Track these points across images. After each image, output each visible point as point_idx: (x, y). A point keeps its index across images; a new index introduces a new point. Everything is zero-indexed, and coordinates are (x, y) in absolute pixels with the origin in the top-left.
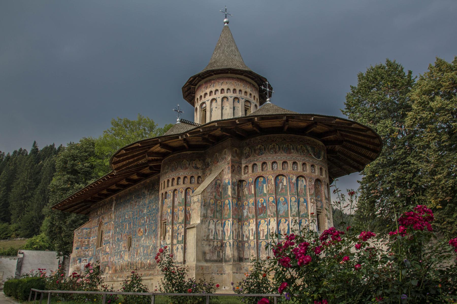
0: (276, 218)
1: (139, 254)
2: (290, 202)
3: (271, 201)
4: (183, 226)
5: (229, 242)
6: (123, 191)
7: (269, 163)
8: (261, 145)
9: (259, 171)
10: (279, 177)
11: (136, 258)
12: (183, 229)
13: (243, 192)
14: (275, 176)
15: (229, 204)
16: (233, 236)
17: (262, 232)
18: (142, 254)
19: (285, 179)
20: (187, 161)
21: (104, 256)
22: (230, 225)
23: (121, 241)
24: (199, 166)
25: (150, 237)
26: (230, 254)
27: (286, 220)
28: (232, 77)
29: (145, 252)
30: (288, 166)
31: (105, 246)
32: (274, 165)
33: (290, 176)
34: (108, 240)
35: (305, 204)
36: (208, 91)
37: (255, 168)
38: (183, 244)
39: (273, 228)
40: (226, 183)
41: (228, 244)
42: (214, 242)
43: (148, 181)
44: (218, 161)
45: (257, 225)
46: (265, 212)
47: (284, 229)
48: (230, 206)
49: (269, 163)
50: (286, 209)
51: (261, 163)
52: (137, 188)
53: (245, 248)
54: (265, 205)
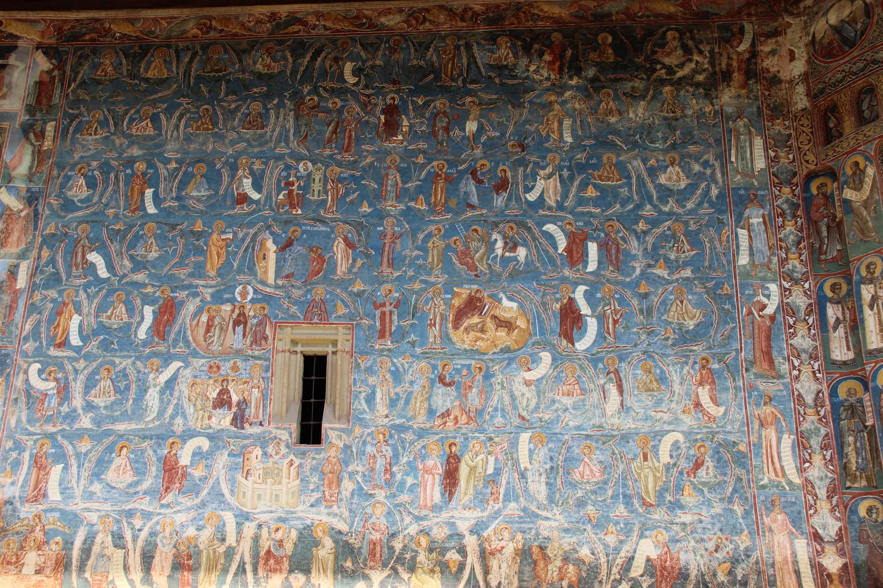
1: (492, 480)
11: (436, 508)
18: (538, 487)
23: (167, 359)
25: (632, 374)
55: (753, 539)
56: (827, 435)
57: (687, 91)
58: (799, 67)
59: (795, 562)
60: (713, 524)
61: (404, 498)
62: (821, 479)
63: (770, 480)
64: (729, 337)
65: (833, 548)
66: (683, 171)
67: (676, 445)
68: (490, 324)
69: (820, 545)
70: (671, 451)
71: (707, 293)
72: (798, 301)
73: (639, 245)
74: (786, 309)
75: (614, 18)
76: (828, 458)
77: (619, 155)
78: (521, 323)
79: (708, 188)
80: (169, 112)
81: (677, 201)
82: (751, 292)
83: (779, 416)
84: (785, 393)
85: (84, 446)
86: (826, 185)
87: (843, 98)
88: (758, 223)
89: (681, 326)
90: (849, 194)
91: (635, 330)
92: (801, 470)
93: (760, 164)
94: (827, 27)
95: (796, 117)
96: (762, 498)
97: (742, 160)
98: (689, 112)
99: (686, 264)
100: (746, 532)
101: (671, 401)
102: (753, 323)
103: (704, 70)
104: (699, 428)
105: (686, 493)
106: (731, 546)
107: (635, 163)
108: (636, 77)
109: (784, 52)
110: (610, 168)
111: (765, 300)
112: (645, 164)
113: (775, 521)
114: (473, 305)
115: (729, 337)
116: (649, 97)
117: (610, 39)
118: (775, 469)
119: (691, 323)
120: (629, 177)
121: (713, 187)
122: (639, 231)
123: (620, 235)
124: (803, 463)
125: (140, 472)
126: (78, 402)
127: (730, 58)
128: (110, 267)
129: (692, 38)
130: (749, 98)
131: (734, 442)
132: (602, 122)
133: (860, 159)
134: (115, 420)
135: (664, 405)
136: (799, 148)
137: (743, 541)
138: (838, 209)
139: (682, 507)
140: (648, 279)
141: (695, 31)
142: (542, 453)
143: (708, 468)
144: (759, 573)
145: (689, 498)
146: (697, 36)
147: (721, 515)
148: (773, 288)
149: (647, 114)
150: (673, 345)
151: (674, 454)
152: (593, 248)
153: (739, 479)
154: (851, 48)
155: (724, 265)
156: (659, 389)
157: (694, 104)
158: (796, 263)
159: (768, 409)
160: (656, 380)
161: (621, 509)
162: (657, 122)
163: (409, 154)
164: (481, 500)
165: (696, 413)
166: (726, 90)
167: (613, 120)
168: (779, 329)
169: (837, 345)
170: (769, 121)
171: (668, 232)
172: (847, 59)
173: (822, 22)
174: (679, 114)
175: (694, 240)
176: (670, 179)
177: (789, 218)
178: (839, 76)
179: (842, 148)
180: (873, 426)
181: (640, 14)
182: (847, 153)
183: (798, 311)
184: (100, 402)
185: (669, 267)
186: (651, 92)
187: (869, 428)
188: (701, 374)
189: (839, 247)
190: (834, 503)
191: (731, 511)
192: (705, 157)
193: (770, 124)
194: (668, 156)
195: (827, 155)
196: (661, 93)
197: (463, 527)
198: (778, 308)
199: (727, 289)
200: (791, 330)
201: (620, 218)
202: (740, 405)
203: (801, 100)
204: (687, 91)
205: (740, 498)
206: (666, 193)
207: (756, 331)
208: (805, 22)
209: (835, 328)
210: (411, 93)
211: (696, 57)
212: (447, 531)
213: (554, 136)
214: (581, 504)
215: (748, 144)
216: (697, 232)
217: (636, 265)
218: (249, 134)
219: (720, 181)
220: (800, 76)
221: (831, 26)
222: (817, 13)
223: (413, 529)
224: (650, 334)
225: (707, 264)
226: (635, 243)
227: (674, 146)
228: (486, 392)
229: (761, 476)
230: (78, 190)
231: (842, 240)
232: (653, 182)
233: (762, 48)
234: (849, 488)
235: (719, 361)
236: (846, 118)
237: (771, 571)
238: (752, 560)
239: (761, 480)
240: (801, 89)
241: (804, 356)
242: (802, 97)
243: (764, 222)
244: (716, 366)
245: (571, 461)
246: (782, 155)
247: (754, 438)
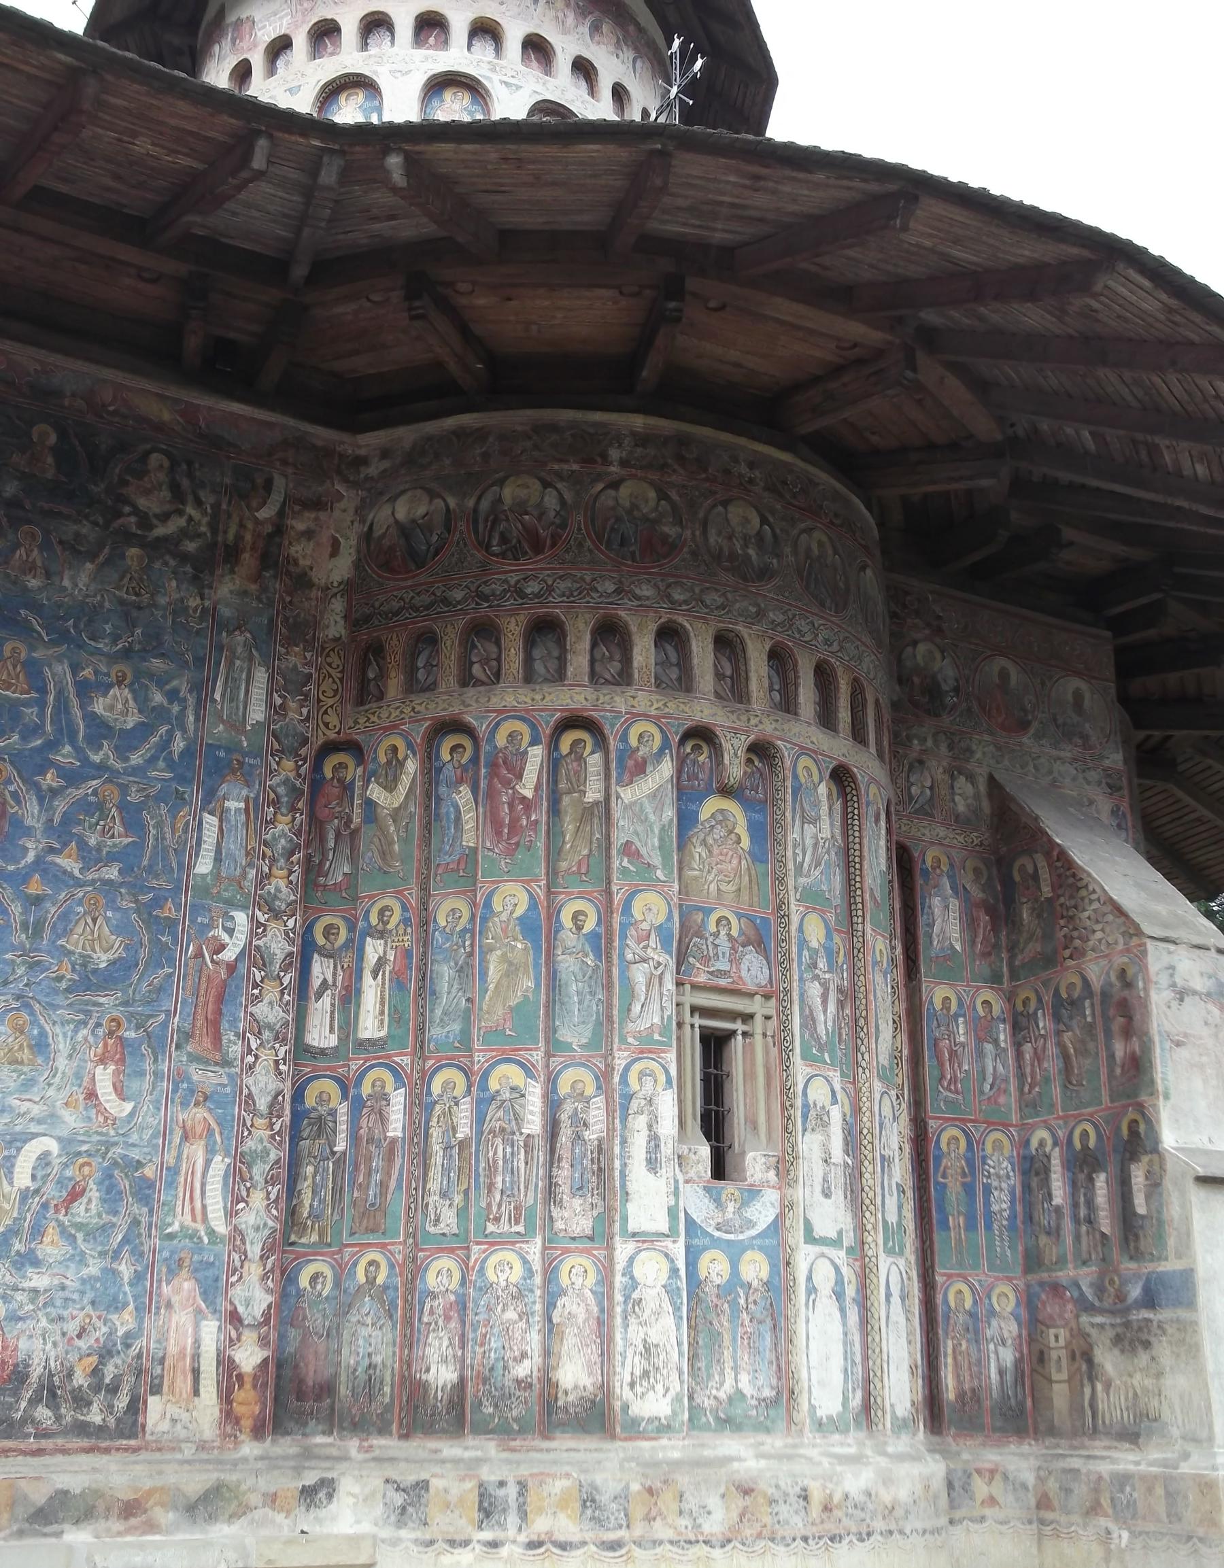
44: (1023, 726)
55: (140, 1320)
56: (277, 1162)
57: (166, 564)
58: (340, 569)
59: (196, 1356)
60: (82, 1293)
62: (257, 1229)
63: (182, 1226)
64: (160, 990)
65: (255, 1335)
66: (135, 699)
67: (44, 1159)
69: (237, 1330)
70: (34, 1168)
71: (138, 911)
72: (274, 945)
73: (40, 812)
74: (254, 955)
75: (66, 402)
76: (273, 1197)
77: (32, 648)
79: (170, 734)
81: (117, 748)
82: (206, 921)
83: (213, 1124)
84: (228, 1089)
86: (346, 767)
87: (395, 642)
88: (237, 810)
89: (86, 960)
90: (376, 792)
91: (8, 956)
92: (231, 1214)
93: (257, 713)
94: (391, 520)
95: (323, 649)
96: (166, 1254)
97: (232, 700)
98: (162, 600)
99: (111, 858)
100: (131, 1307)
101: (49, 1085)
102: (200, 971)
103: (199, 535)
104: (86, 1133)
105: (46, 1240)
106: (104, 1329)
107: (58, 668)
108: (86, 517)
110: (15, 667)
111: (225, 937)
112: (74, 674)
113: (178, 1291)
115: (160, 990)
116: (101, 558)
117: (53, 438)
118: (193, 1210)
119: (104, 957)
120: (43, 691)
121: (178, 734)
122: (44, 787)
123: (12, 788)
124: (235, 1200)
127: (242, 525)
129: (190, 475)
130: (259, 600)
131: (138, 1162)
132: (15, 583)
133: (400, 743)
135: (36, 1089)
136: (319, 701)
137: (124, 1322)
138: (357, 811)
139: (36, 1263)
140: (44, 872)
141: (197, 466)
143: (90, 1200)
144: (139, 1373)
145: (51, 1248)
146: (198, 474)
147: (97, 1279)
149: (93, 587)
150: (68, 990)
151: (39, 1174)
153: (136, 1223)
154: (419, 567)
155: (172, 869)
156: (32, 1062)
157: (172, 590)
158: (282, 884)
159: (200, 1113)
160: (30, 1047)
162: (107, 604)
165: (86, 1109)
166: (227, 578)
167: (33, 583)
168: (237, 987)
169: (317, 1022)
170: (282, 646)
171: (93, 799)
172: (409, 583)
173: (386, 511)
174: (146, 598)
175: (133, 820)
176: (111, 708)
177: (284, 810)
178: (395, 605)
179: (379, 718)
180: (344, 1153)
181: (111, 408)
182: (386, 729)
183: (271, 963)
185: (83, 858)
186: (106, 550)
187: (338, 1155)
188: (106, 1045)
189: (347, 870)
190: (269, 1266)
191: (115, 1272)
192: (175, 683)
193: (283, 650)
194: (116, 667)
195: (356, 722)
196: (123, 557)
198: (242, 952)
199: (168, 911)
200: (256, 991)
201: (17, 759)
202: (158, 1101)
203: (335, 626)
204: (166, 564)
205: (132, 1252)
206: (100, 729)
207: (203, 986)
208: (363, 500)
209: (319, 995)
211: (190, 510)
215: (244, 676)
216: (140, 807)
217: (29, 845)
219: (191, 727)
220: (340, 584)
221: (397, 522)
222: (381, 493)
224: (33, 966)
225: (145, 862)
226: (33, 807)
227: (127, 653)
229: (169, 1220)
231: (353, 861)
232: (82, 707)
233: (294, 523)
234: (293, 1244)
235: (138, 1027)
236: (393, 674)
237: (158, 1370)
238: (133, 1352)
239: (170, 1225)
240: (338, 605)
241: (267, 1034)
242: (338, 619)
243: (247, 810)
244: (131, 1034)
246: (293, 705)
247: (170, 1158)
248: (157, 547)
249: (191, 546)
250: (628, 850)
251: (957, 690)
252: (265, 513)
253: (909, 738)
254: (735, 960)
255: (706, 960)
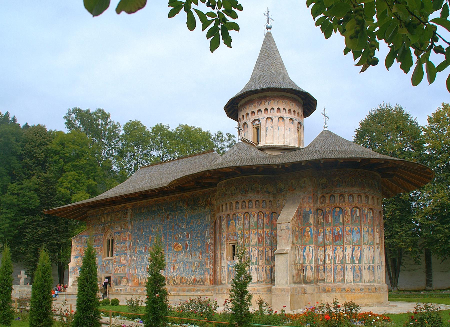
0: (351, 246)
1: (178, 269)
2: (363, 231)
3: (348, 230)
4: (256, 249)
5: (311, 266)
6: (144, 201)
7: (346, 195)
8: (339, 178)
9: (336, 202)
10: (354, 209)
11: (172, 273)
12: (257, 251)
13: (318, 220)
14: (352, 208)
15: (311, 231)
16: (314, 261)
17: (337, 257)
19: (358, 211)
20: (259, 185)
21: (117, 267)
22: (311, 251)
23: (146, 254)
24: (270, 190)
25: (193, 254)
26: (312, 276)
27: (359, 248)
28: (287, 97)
29: (187, 267)
30: (361, 199)
31: (117, 256)
32: (349, 198)
33: (363, 209)
34: (124, 251)
35: (372, 233)
36: (262, 109)
37: (331, 199)
38: (257, 265)
39: (349, 254)
40: (306, 211)
41: (309, 268)
42: (298, 265)
43: (187, 194)
44: (295, 189)
45: (334, 251)
46: (340, 240)
47: (357, 255)
48: (311, 233)
49: (346, 195)
50: (359, 238)
51: (339, 195)
52: (168, 199)
53: (320, 270)
54: (341, 234)
61: (169, 271)
68: (178, 247)
74: (210, 243)
78: (181, 247)
80: (144, 218)
85: (139, 266)
92: (210, 266)
93: (209, 220)
109: (214, 200)
114: (176, 245)
125: (144, 269)
126: (138, 261)
128: (140, 242)
134: (142, 263)
137: (203, 276)
142: (183, 265)
145: (197, 271)
148: (209, 240)
152: (189, 235)
161: (190, 272)
163: (170, 222)
164: (177, 272)
184: (140, 261)
197: (175, 275)
210: (170, 212)
211: (204, 202)
212: (173, 276)
213: (186, 218)
214: (186, 272)
218: (153, 220)
223: (170, 276)
228: (177, 257)
230: (136, 231)
245: (186, 266)
248: (201, 207)
249: (204, 205)
250: (223, 229)
251: (284, 188)
252: (209, 199)
253: (277, 198)
254: (233, 238)
255: (230, 238)
